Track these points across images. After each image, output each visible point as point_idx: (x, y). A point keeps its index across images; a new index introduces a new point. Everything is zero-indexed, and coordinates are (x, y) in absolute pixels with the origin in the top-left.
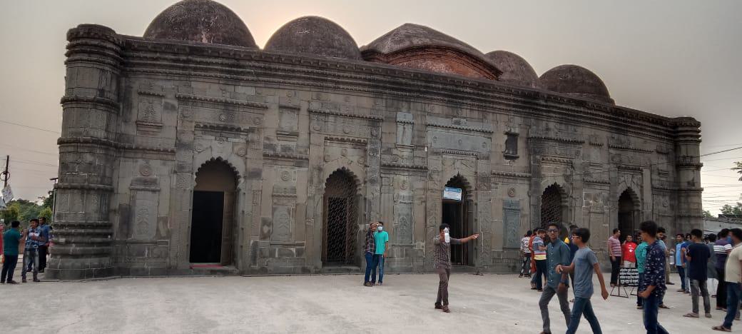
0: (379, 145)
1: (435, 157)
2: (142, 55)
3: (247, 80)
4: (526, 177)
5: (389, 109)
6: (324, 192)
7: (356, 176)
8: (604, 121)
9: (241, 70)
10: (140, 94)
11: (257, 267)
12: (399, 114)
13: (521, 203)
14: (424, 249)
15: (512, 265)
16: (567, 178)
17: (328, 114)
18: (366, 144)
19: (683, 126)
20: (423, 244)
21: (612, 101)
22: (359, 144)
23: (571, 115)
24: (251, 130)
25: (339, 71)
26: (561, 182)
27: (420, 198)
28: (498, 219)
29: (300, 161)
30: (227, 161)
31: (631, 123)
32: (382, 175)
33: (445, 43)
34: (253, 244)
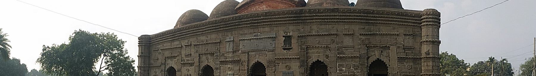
1: (244, 54)
8: (357, 19)
16: (327, 57)
23: (327, 19)
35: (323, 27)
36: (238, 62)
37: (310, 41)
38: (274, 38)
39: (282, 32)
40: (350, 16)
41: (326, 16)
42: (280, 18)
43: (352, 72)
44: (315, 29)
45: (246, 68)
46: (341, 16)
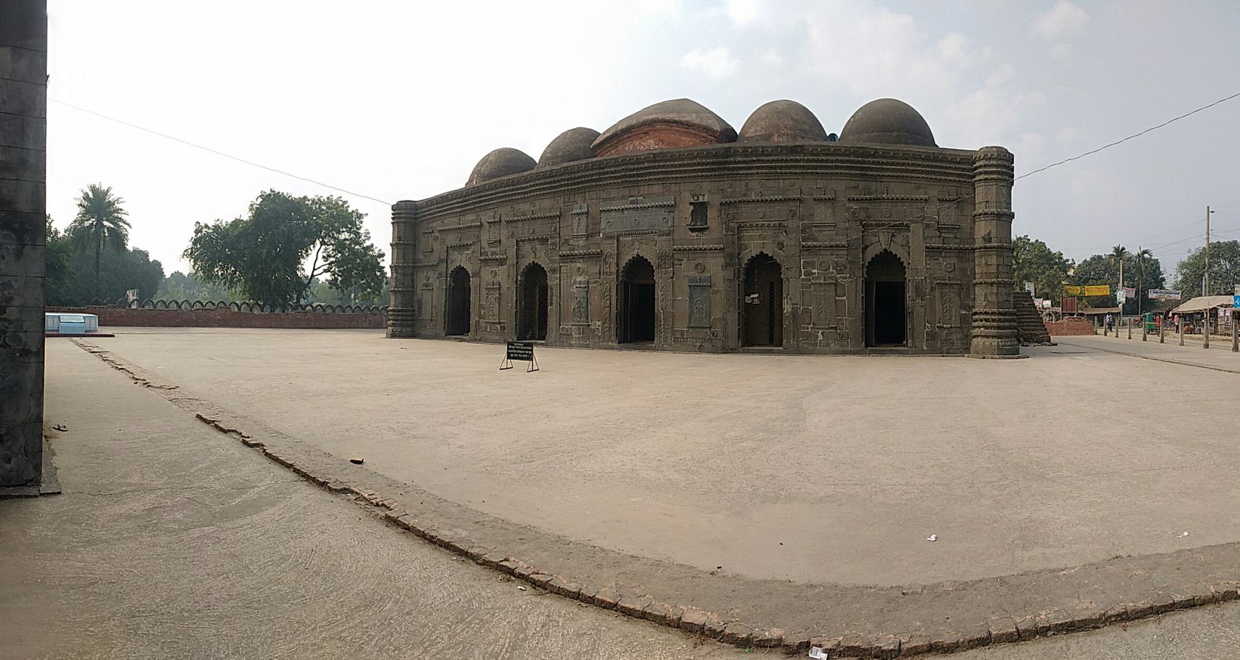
8: (842, 168)
13: (713, 279)
16: (781, 246)
23: (781, 168)
28: (683, 298)
29: (501, 262)
35: (771, 183)
36: (597, 256)
37: (747, 214)
38: (671, 208)
39: (688, 195)
40: (827, 161)
41: (778, 161)
42: (685, 165)
43: (831, 278)
44: (756, 187)
45: (614, 269)
46: (808, 161)
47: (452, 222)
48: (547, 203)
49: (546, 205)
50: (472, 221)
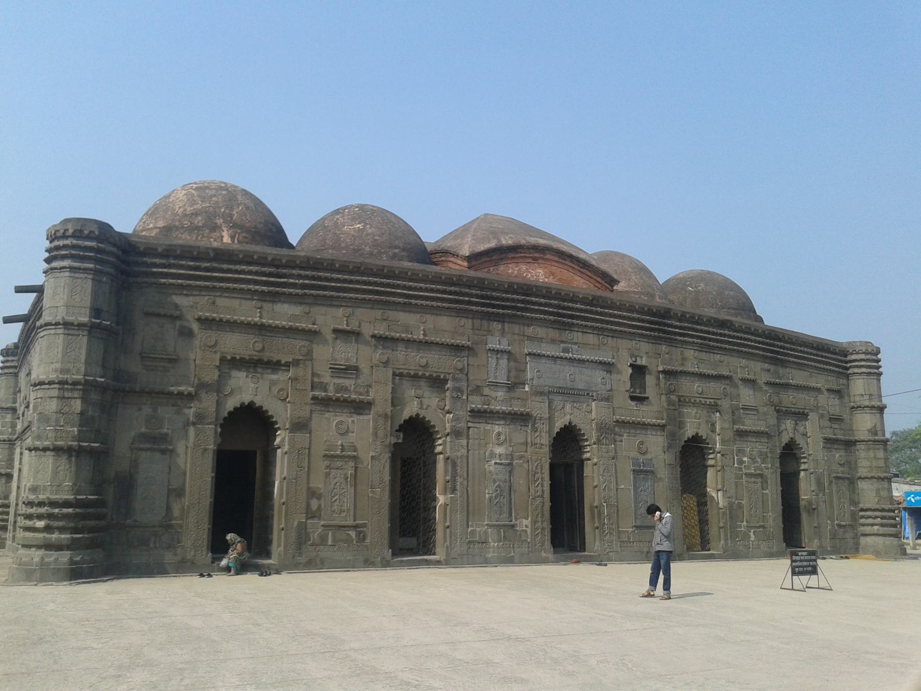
0: (465, 384)
1: (538, 398)
2: (148, 260)
3: (290, 294)
4: (659, 425)
5: (477, 332)
6: (392, 449)
7: (434, 426)
9: (283, 280)
10: (148, 314)
11: (303, 559)
12: (490, 338)
14: (529, 531)
15: (645, 550)
17: (397, 339)
18: (445, 381)
19: (857, 353)
20: (525, 522)
21: (760, 320)
22: (437, 383)
23: (710, 340)
24: (296, 363)
25: (411, 280)
26: (703, 433)
27: (521, 457)
29: (360, 407)
30: (261, 407)
31: (791, 350)
32: (470, 424)
33: (542, 242)
34: (298, 526)
35: (703, 356)
38: (608, 367)
47: (245, 310)
48: (445, 322)
49: (445, 327)
50: (294, 317)
